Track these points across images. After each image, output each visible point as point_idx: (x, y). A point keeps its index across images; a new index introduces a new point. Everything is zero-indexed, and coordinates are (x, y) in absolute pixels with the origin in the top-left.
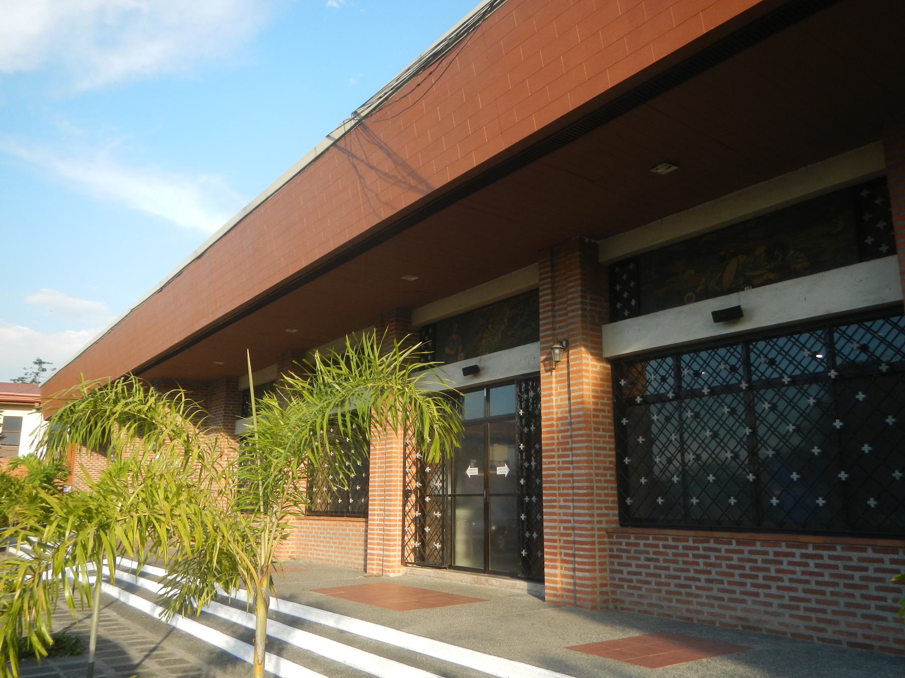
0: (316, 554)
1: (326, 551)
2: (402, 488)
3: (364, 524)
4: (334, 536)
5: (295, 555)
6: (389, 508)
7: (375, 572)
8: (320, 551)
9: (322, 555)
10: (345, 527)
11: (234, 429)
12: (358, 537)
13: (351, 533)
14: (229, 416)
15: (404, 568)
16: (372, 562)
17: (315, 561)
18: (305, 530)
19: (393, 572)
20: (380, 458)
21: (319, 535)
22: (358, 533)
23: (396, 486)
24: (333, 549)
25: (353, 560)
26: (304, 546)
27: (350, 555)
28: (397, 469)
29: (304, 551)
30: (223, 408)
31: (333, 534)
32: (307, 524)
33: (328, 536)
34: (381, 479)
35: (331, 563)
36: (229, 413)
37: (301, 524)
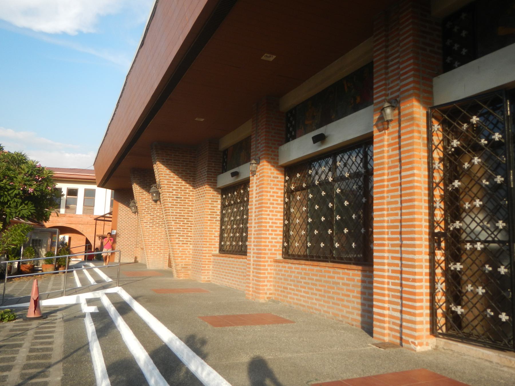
0: (297, 299)
1: (308, 298)
2: (427, 230)
3: (360, 273)
4: (318, 283)
5: (273, 297)
6: (411, 256)
7: (387, 339)
8: (301, 296)
9: (304, 301)
10: (331, 274)
11: (216, 183)
12: (351, 288)
13: (341, 281)
14: (212, 172)
15: (433, 341)
16: (382, 325)
17: (295, 306)
18: (283, 273)
19: (421, 344)
20: (388, 191)
21: (299, 279)
22: (351, 283)
23: (420, 226)
24: (317, 297)
25: (344, 313)
26: (282, 289)
27: (340, 307)
28: (420, 204)
29: (283, 294)
30: (207, 165)
31: (317, 280)
32: (285, 267)
33: (310, 281)
34: (392, 218)
35: (315, 311)
36: (212, 169)
37: (279, 266)
